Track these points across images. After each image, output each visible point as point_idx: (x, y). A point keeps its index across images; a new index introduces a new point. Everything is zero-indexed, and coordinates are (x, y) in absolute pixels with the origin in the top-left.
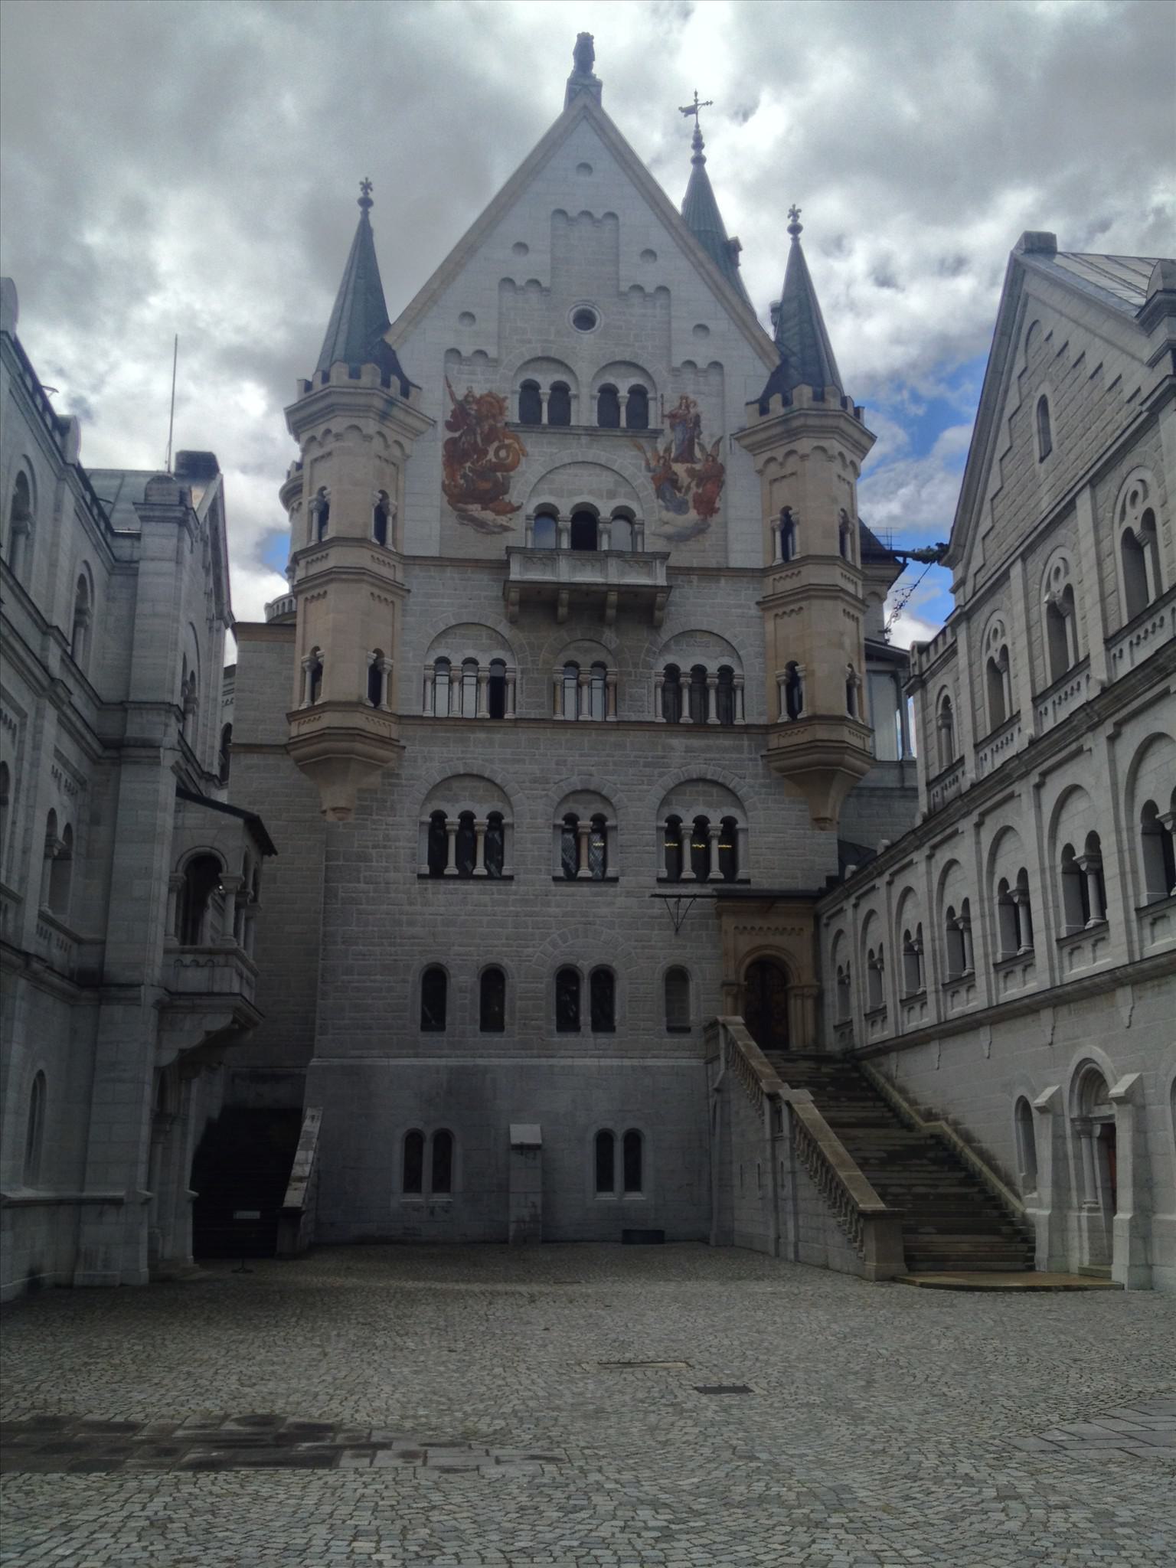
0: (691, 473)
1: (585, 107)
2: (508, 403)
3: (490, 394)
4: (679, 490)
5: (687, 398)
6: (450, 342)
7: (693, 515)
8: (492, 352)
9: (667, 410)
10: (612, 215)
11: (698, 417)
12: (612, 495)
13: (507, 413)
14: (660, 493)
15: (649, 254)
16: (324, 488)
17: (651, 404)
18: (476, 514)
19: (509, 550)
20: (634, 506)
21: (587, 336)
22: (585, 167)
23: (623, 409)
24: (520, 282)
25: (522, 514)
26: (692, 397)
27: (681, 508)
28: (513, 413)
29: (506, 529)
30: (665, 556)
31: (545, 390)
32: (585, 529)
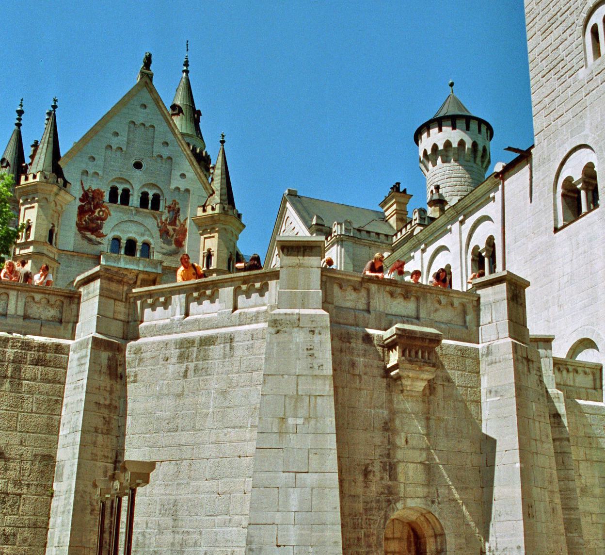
0: (174, 230)
1: (146, 82)
2: (105, 194)
3: (98, 190)
4: (169, 236)
5: (175, 201)
6: (83, 166)
7: (174, 246)
8: (100, 173)
9: (167, 205)
10: (153, 126)
11: (179, 209)
12: (143, 235)
13: (104, 198)
14: (161, 236)
15: (166, 144)
16: (30, 220)
17: (161, 202)
18: (89, 236)
19: (101, 253)
20: (151, 240)
21: (138, 172)
22: (144, 106)
23: (150, 202)
24: (114, 147)
25: (106, 238)
26: (177, 201)
27: (169, 243)
28: (106, 197)
29: (100, 243)
30: (161, 262)
31: (120, 192)
32: (131, 247)
